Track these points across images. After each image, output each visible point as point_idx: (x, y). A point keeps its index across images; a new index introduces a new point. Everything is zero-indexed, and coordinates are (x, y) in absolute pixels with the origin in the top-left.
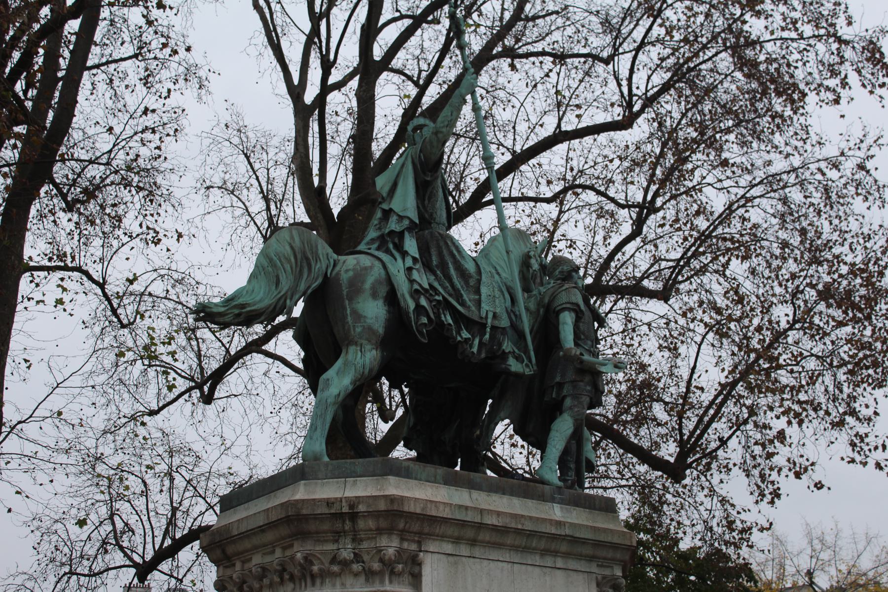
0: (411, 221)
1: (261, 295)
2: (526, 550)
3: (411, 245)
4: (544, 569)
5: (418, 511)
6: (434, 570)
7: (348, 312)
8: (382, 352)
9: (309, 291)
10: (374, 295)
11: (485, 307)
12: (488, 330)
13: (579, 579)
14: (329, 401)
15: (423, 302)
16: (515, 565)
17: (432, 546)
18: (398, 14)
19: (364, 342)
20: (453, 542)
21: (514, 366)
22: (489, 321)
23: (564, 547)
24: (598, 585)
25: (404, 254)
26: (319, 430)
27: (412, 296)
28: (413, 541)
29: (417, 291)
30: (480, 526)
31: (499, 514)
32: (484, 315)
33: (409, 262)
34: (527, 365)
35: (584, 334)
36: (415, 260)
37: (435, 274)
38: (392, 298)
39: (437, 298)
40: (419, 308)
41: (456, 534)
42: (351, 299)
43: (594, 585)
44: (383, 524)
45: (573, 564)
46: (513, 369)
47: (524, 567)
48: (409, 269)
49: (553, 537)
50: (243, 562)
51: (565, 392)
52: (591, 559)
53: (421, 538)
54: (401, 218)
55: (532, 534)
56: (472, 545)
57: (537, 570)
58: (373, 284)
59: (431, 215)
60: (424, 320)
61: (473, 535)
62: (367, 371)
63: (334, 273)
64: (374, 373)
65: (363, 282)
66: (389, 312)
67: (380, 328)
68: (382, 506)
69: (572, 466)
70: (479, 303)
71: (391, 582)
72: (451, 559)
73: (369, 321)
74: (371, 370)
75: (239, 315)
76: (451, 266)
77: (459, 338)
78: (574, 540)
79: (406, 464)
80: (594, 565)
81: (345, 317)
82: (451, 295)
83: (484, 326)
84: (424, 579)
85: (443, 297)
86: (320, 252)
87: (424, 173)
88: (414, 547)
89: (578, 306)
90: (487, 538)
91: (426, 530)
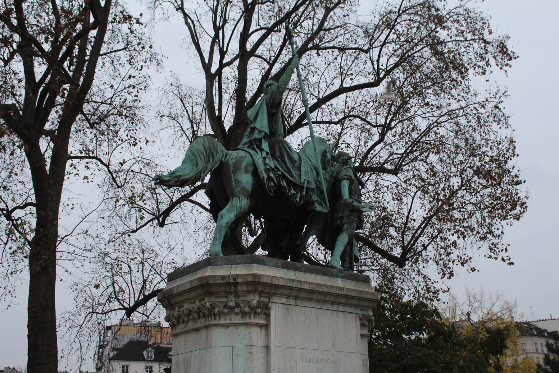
0: (265, 133)
1: (188, 171)
2: (323, 302)
3: (265, 146)
4: (333, 312)
5: (269, 282)
6: (276, 311)
7: (233, 180)
9: (213, 169)
10: (246, 171)
11: (303, 177)
12: (305, 189)
14: (223, 225)
15: (272, 175)
17: (275, 300)
18: (259, 27)
19: (241, 195)
20: (286, 298)
21: (318, 208)
22: (305, 185)
23: (343, 301)
24: (360, 320)
25: (262, 150)
26: (218, 240)
27: (266, 172)
28: (266, 297)
29: (268, 169)
30: (300, 290)
31: (310, 283)
33: (264, 154)
34: (324, 208)
36: (267, 153)
37: (277, 160)
38: (255, 173)
39: (279, 173)
40: (269, 178)
41: (288, 293)
42: (234, 173)
43: (358, 320)
44: (251, 288)
45: (347, 309)
46: (317, 209)
47: (322, 310)
48: (264, 158)
49: (338, 295)
50: (180, 307)
51: (344, 221)
52: (357, 306)
53: (270, 295)
54: (260, 132)
55: (327, 294)
56: (296, 299)
57: (329, 312)
58: (245, 165)
59: (276, 130)
60: (272, 184)
61: (297, 294)
62: (242, 210)
63: (226, 160)
64: (246, 211)
65: (241, 164)
66: (254, 180)
67: (249, 188)
68: (250, 279)
69: (348, 259)
70: (300, 175)
71: (254, 318)
72: (285, 306)
73: (243, 184)
74: (244, 210)
75: (177, 181)
76: (285, 156)
77: (290, 194)
78: (348, 297)
79: (263, 258)
80: (358, 309)
81: (231, 182)
82: (285, 171)
83: (303, 187)
84: (271, 316)
85: (282, 172)
86: (218, 149)
87: (272, 109)
88: (266, 300)
89: (351, 177)
90: (304, 296)
91: (273, 291)
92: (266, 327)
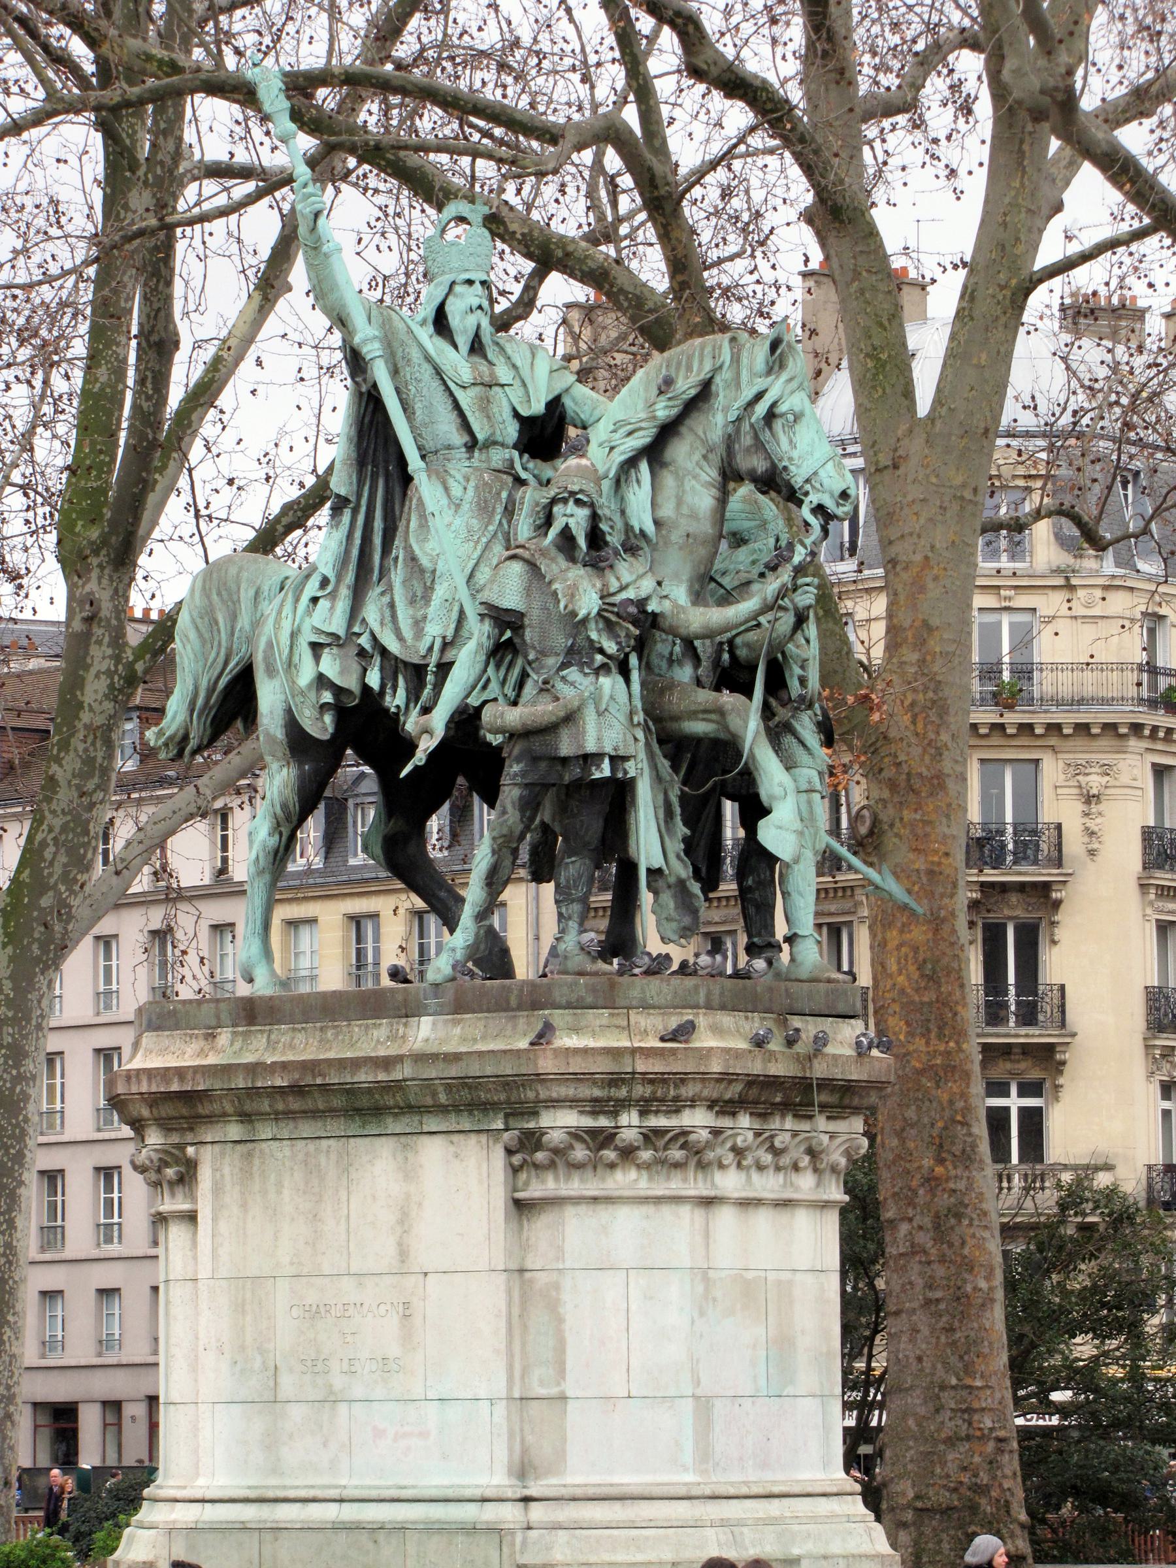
4: (403, 1139)
8: (300, 768)
9: (222, 684)
10: (271, 672)
13: (472, 1146)
15: (330, 666)
16: (352, 1140)
24: (509, 1152)
32: (423, 652)
43: (499, 1153)
53: (194, 1122)
70: (419, 625)
71: (173, 1195)
74: (284, 806)
75: (166, 745)
92: (191, 1217)
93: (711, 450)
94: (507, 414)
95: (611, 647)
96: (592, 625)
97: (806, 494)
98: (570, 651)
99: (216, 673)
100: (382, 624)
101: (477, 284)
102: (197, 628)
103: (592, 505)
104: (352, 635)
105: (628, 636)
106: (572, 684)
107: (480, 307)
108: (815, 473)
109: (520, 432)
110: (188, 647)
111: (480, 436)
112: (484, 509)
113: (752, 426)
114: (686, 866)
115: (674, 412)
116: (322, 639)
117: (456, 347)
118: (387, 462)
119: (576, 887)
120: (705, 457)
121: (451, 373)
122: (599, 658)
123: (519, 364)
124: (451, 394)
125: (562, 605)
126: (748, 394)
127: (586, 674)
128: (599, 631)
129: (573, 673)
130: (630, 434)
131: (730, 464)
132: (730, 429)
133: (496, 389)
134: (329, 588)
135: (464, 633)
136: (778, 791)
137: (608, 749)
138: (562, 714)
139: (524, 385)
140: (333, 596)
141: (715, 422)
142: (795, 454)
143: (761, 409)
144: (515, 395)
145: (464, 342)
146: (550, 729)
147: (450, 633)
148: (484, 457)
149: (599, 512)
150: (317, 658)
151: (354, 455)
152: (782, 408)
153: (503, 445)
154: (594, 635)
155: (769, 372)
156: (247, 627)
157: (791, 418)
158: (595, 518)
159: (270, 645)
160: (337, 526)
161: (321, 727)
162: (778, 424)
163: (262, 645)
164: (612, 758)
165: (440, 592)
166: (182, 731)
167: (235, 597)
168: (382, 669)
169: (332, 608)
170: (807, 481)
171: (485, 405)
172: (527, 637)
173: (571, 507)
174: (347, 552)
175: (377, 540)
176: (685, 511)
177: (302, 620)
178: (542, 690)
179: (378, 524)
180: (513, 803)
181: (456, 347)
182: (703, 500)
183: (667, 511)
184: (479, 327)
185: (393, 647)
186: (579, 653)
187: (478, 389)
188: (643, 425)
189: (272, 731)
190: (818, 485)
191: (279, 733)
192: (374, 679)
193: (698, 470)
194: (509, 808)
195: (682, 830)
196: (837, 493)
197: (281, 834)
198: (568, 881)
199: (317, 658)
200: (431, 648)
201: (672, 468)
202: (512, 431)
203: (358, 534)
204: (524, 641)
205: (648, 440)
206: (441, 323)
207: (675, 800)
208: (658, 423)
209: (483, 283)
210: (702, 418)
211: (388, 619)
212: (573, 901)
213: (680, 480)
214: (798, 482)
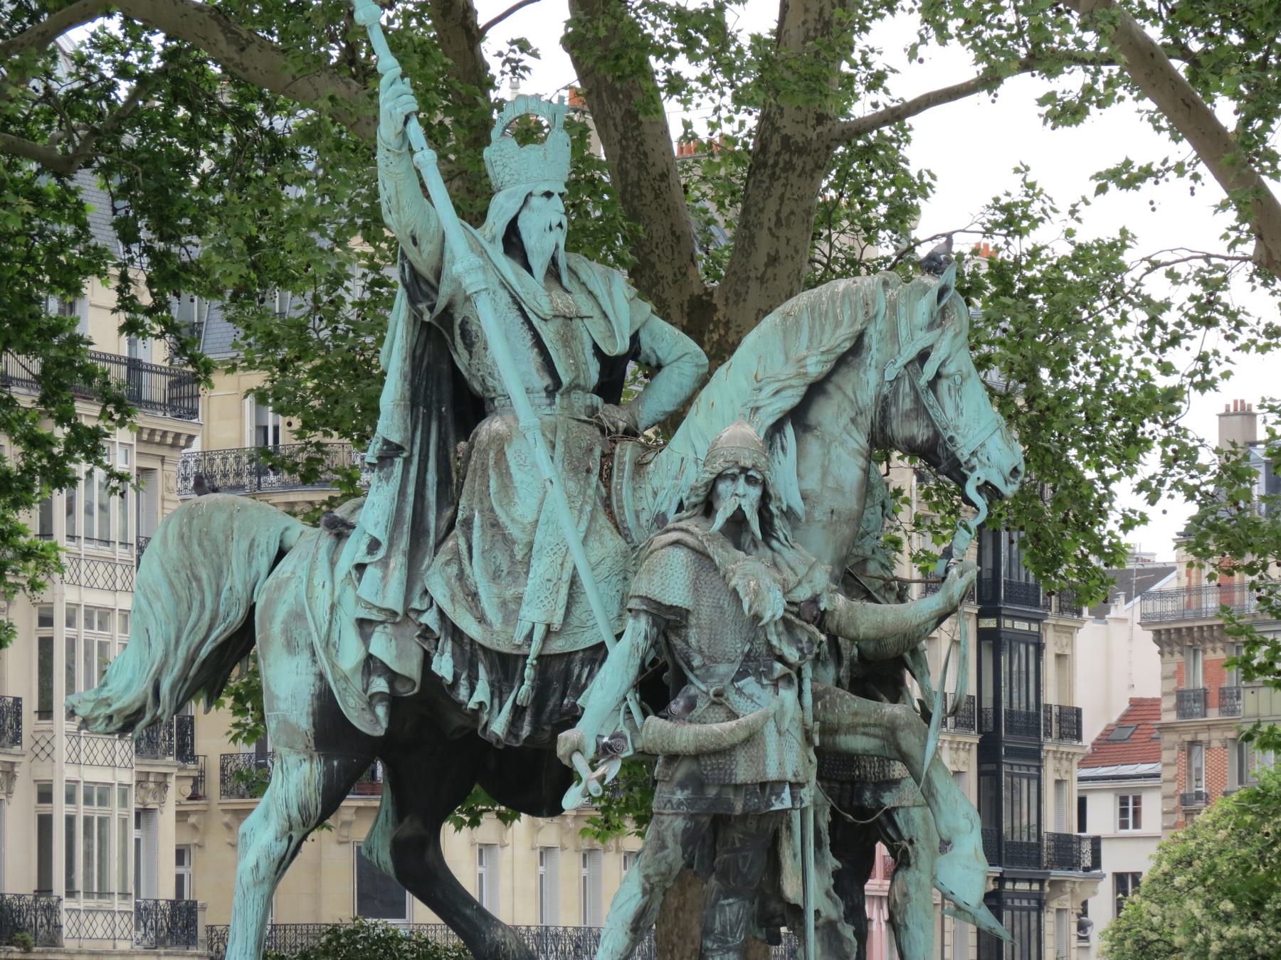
8: (327, 759)
9: (204, 652)
10: (291, 646)
12: (529, 672)
15: (381, 646)
32: (519, 640)
35: (701, 652)
58: (285, 622)
62: (295, 813)
70: (510, 609)
74: (303, 808)
85: (441, 613)
93: (860, 412)
94: (589, 351)
95: (792, 654)
96: (772, 628)
97: (972, 469)
98: (748, 657)
99: (197, 640)
100: (453, 600)
101: (556, 198)
102: (171, 585)
103: (764, 485)
104: (407, 611)
105: (810, 641)
106: (750, 697)
107: (560, 225)
108: (983, 445)
109: (601, 373)
110: (157, 606)
111: (565, 379)
112: (577, 468)
113: (913, 387)
114: (836, 904)
115: (828, 367)
116: (374, 616)
117: (529, 269)
118: (440, 402)
119: (733, 935)
120: (853, 421)
121: (533, 304)
122: (778, 666)
123: (597, 292)
124: (532, 327)
125: (746, 607)
126: (910, 352)
127: (763, 686)
128: (778, 635)
129: (749, 684)
130: (777, 392)
131: (882, 430)
132: (885, 390)
133: (578, 321)
134: (381, 553)
135: (574, 621)
136: (963, 824)
137: (790, 777)
138: (742, 735)
139: (605, 315)
140: (384, 563)
141: (866, 384)
142: (962, 421)
143: (930, 370)
144: (596, 329)
145: (539, 263)
146: (723, 752)
147: (557, 621)
148: (565, 402)
149: (771, 492)
150: (366, 639)
151: (408, 394)
152: (951, 369)
153: (584, 389)
154: (775, 641)
155: (931, 326)
156: (239, 587)
157: (958, 378)
158: (765, 498)
159: (297, 616)
160: (388, 478)
161: (371, 722)
162: (944, 385)
163: (281, 612)
164: (791, 785)
165: (541, 568)
166: (137, 705)
167: (222, 550)
168: (453, 655)
169: (384, 578)
170: (974, 454)
171: (567, 340)
172: (693, 641)
173: (741, 484)
174: (399, 510)
175: (431, 496)
176: (830, 482)
177: (343, 590)
178: (714, 703)
179: (432, 477)
180: (674, 835)
181: (529, 269)
182: (849, 470)
183: (812, 483)
184: (557, 247)
185: (471, 629)
186: (757, 663)
187: (560, 321)
188: (793, 382)
189: (293, 719)
190: (984, 459)
191: (304, 722)
192: (444, 666)
193: (845, 436)
194: (670, 842)
195: (832, 863)
196: (1007, 470)
197: (290, 838)
198: (724, 927)
199: (366, 639)
200: (529, 637)
201: (817, 433)
202: (593, 371)
203: (411, 490)
204: (687, 643)
205: (797, 400)
206: (513, 242)
207: (824, 826)
208: (809, 380)
209: (561, 195)
210: (852, 375)
211: (460, 595)
212: (729, 950)
213: (826, 446)
214: (963, 454)
